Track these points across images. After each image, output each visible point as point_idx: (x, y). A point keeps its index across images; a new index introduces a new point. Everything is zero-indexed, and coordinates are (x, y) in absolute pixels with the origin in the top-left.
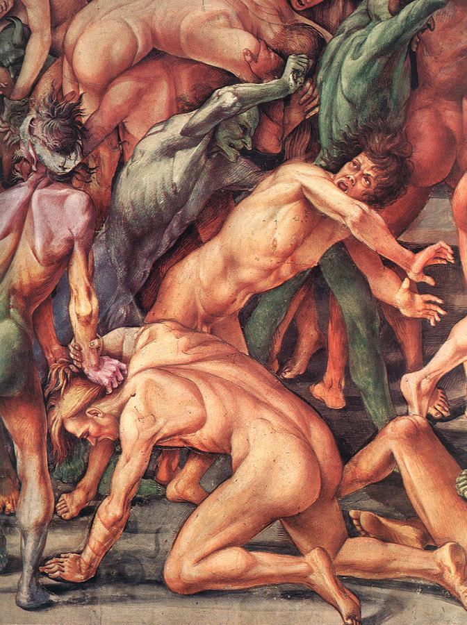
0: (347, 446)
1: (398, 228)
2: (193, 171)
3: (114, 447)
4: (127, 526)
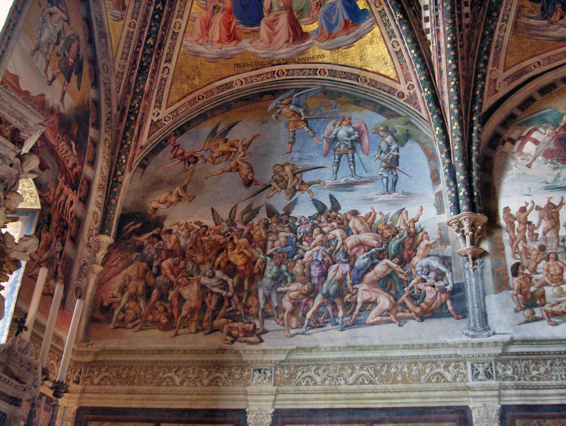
0: (396, 300)
1: (402, 268)
2: (368, 261)
3: (356, 303)
4: (359, 315)
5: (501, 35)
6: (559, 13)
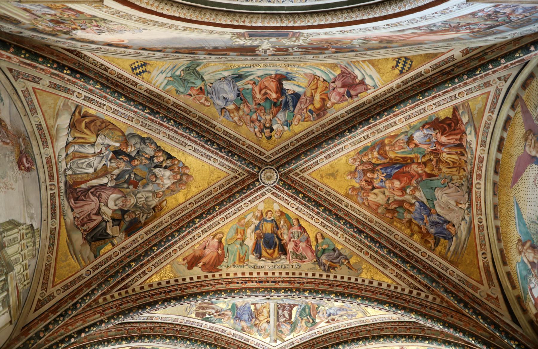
5: (456, 276)
6: (450, 227)
